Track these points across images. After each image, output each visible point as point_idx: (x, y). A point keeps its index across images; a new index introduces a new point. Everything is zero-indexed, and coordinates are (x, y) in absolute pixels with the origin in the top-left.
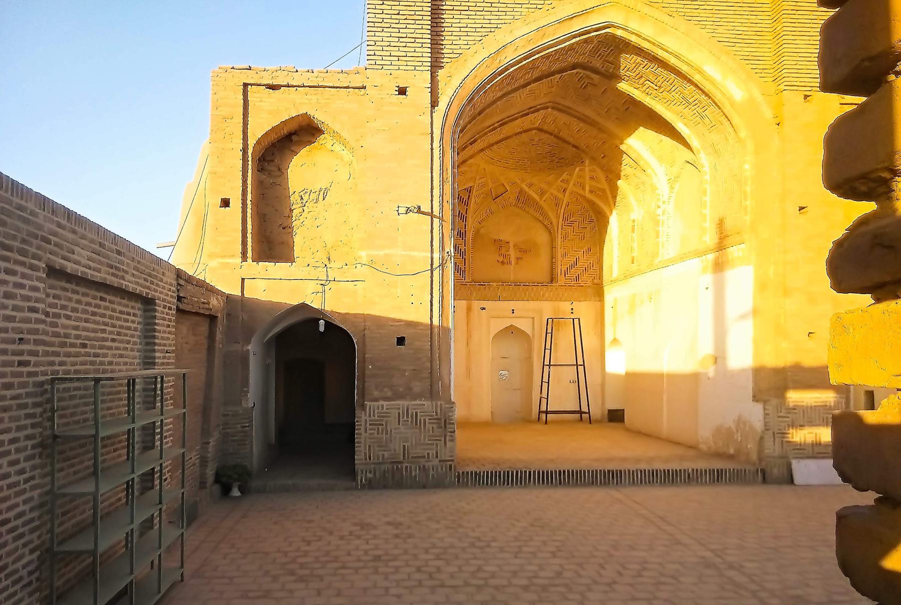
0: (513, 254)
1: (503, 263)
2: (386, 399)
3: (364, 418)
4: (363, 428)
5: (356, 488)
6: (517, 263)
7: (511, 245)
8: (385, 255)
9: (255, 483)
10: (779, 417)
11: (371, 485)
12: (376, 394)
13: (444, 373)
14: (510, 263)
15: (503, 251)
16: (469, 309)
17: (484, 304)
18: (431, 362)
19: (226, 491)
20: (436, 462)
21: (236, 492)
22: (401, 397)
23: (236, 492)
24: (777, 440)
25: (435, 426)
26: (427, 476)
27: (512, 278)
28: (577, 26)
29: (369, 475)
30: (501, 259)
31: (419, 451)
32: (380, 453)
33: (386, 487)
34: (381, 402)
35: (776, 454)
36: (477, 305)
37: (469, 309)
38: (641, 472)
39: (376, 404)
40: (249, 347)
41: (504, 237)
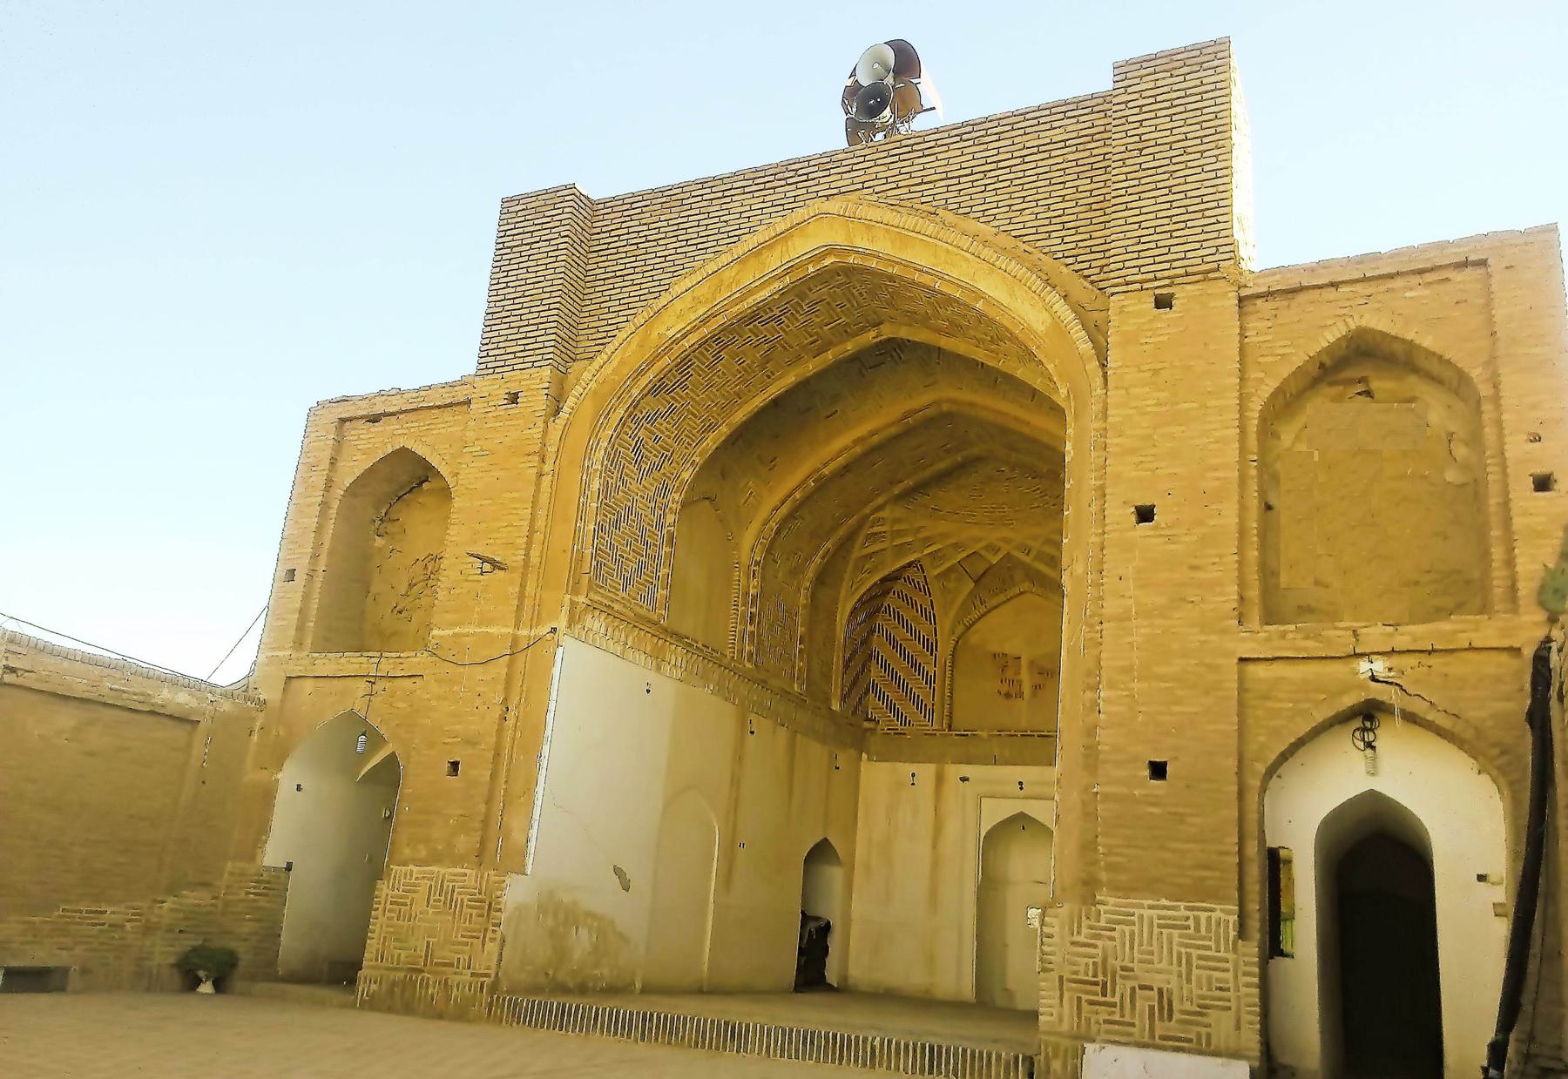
0: (1025, 676)
1: (1008, 695)
2: (419, 862)
3: (385, 891)
4: (381, 907)
5: (353, 1006)
6: (1034, 695)
7: (1024, 662)
8: (455, 635)
9: (238, 984)
10: (1073, 943)
11: (373, 1004)
12: (407, 852)
13: (515, 823)
14: (1021, 695)
15: (1009, 674)
16: (940, 779)
17: (966, 770)
18: (489, 801)
19: (192, 983)
20: (467, 977)
21: (206, 988)
22: (435, 858)
23: (206, 988)
24: (1066, 995)
25: (474, 912)
26: (448, 998)
27: (1024, 724)
28: (774, 261)
29: (374, 987)
30: (1004, 688)
31: (443, 955)
32: (396, 952)
33: (390, 1010)
34: (411, 867)
35: (1065, 1027)
36: (954, 771)
37: (940, 779)
38: (784, 1031)
39: (404, 869)
40: (279, 776)
41: (1011, 648)
